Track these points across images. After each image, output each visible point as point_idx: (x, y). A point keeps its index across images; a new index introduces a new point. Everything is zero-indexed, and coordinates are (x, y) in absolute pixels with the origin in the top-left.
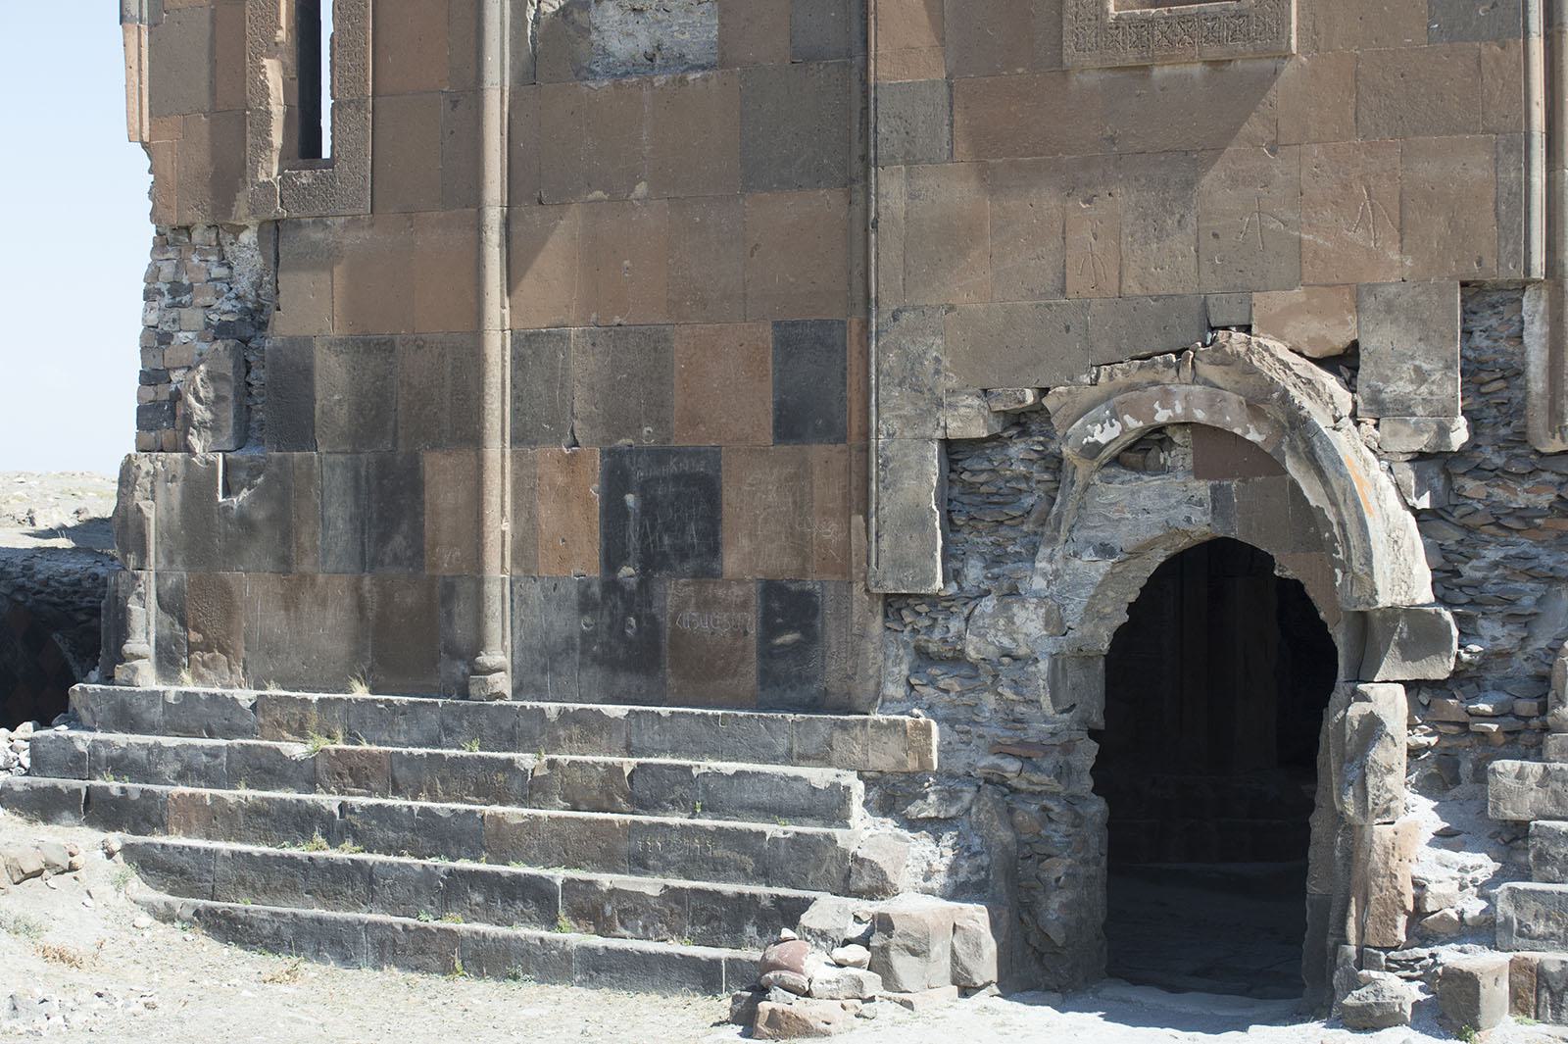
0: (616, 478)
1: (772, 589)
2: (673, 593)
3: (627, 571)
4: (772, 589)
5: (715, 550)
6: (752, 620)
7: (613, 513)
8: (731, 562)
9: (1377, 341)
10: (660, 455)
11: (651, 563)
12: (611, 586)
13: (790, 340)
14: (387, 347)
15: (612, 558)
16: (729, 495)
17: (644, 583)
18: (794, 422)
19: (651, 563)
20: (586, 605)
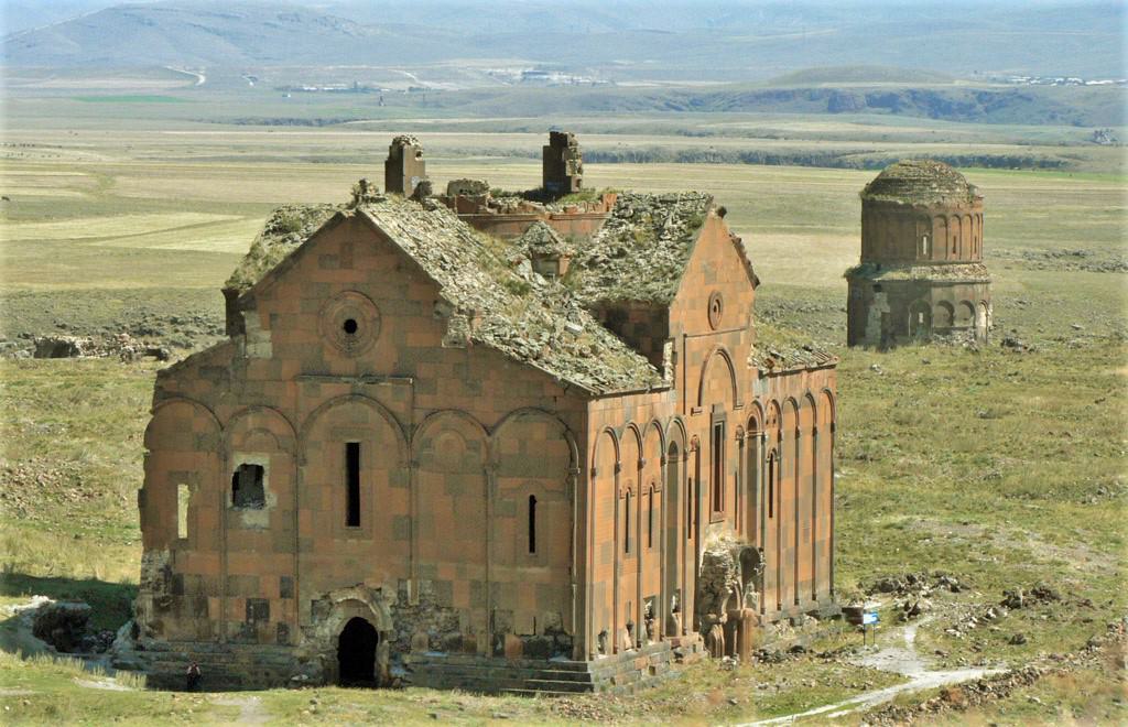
0: (249, 602)
1: (279, 624)
2: (260, 625)
3: (251, 621)
4: (279, 624)
5: (268, 615)
6: (276, 630)
7: (248, 611)
8: (272, 619)
9: (384, 587)
10: (258, 599)
11: (256, 618)
12: (248, 623)
13: (283, 580)
14: (200, 576)
15: (248, 618)
16: (271, 606)
17: (255, 622)
18: (283, 595)
19: (256, 618)
20: (243, 626)
